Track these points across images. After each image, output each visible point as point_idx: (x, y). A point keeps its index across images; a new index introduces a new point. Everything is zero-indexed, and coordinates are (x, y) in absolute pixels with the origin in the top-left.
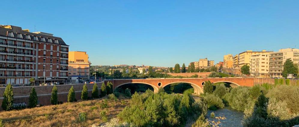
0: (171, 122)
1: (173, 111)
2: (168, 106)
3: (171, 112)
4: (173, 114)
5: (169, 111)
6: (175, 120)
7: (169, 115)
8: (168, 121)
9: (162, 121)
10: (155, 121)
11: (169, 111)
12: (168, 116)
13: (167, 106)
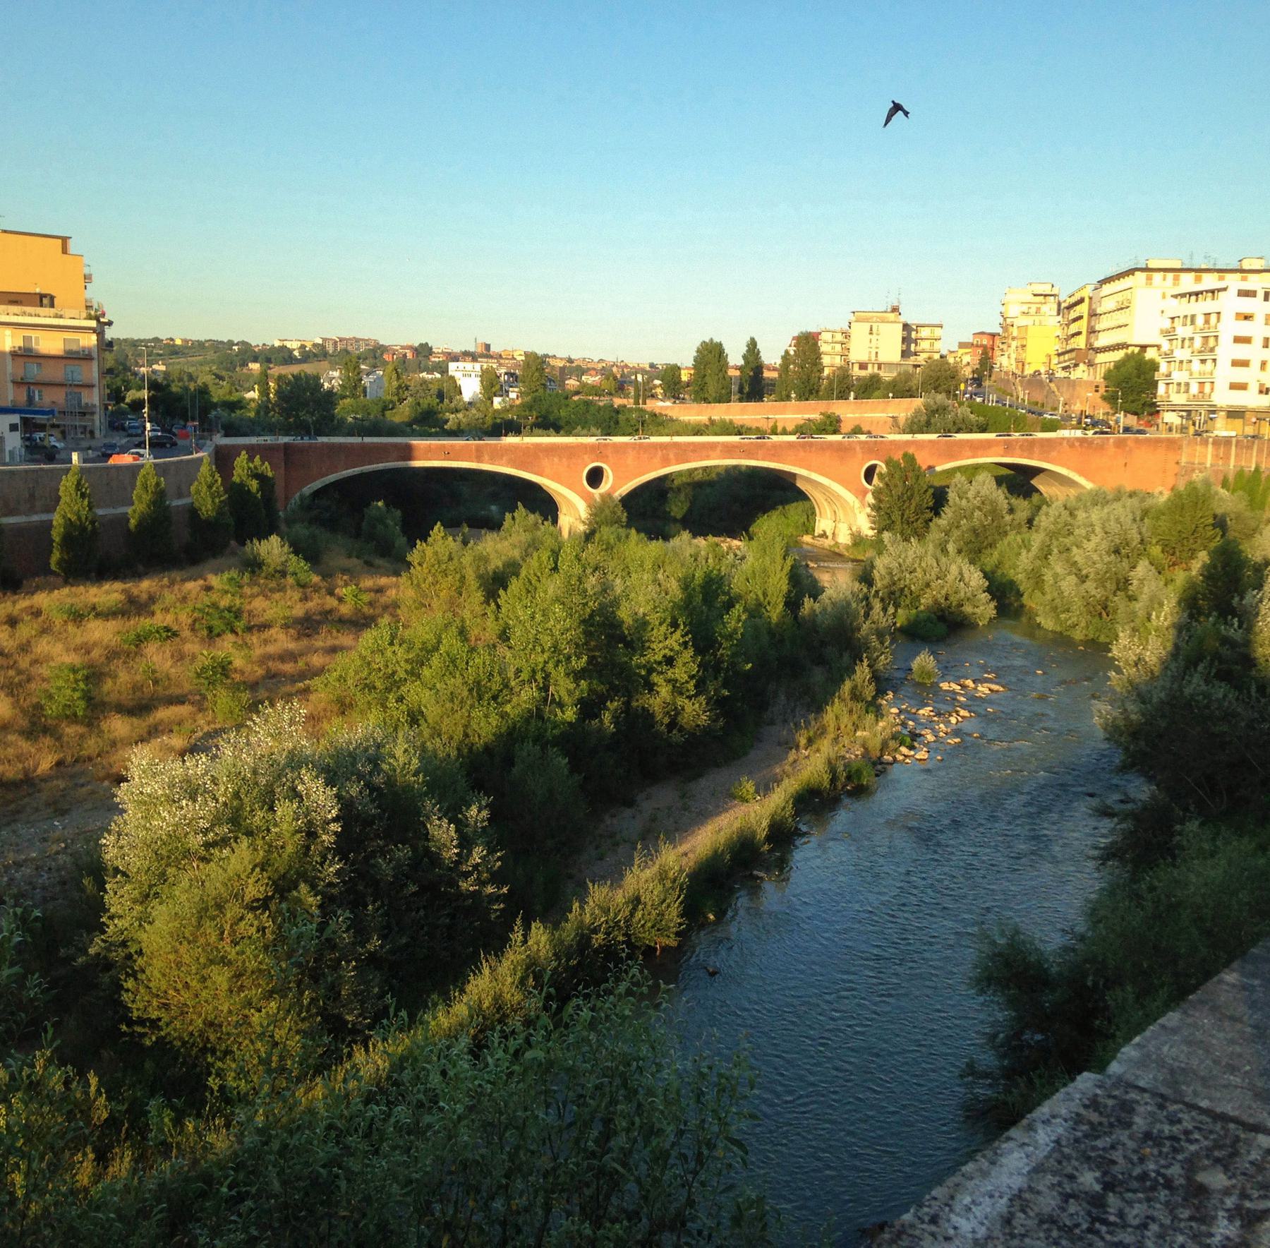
0: (666, 720)
3: (670, 661)
6: (695, 712)
7: (655, 678)
8: (647, 715)
10: (570, 714)
12: (650, 687)
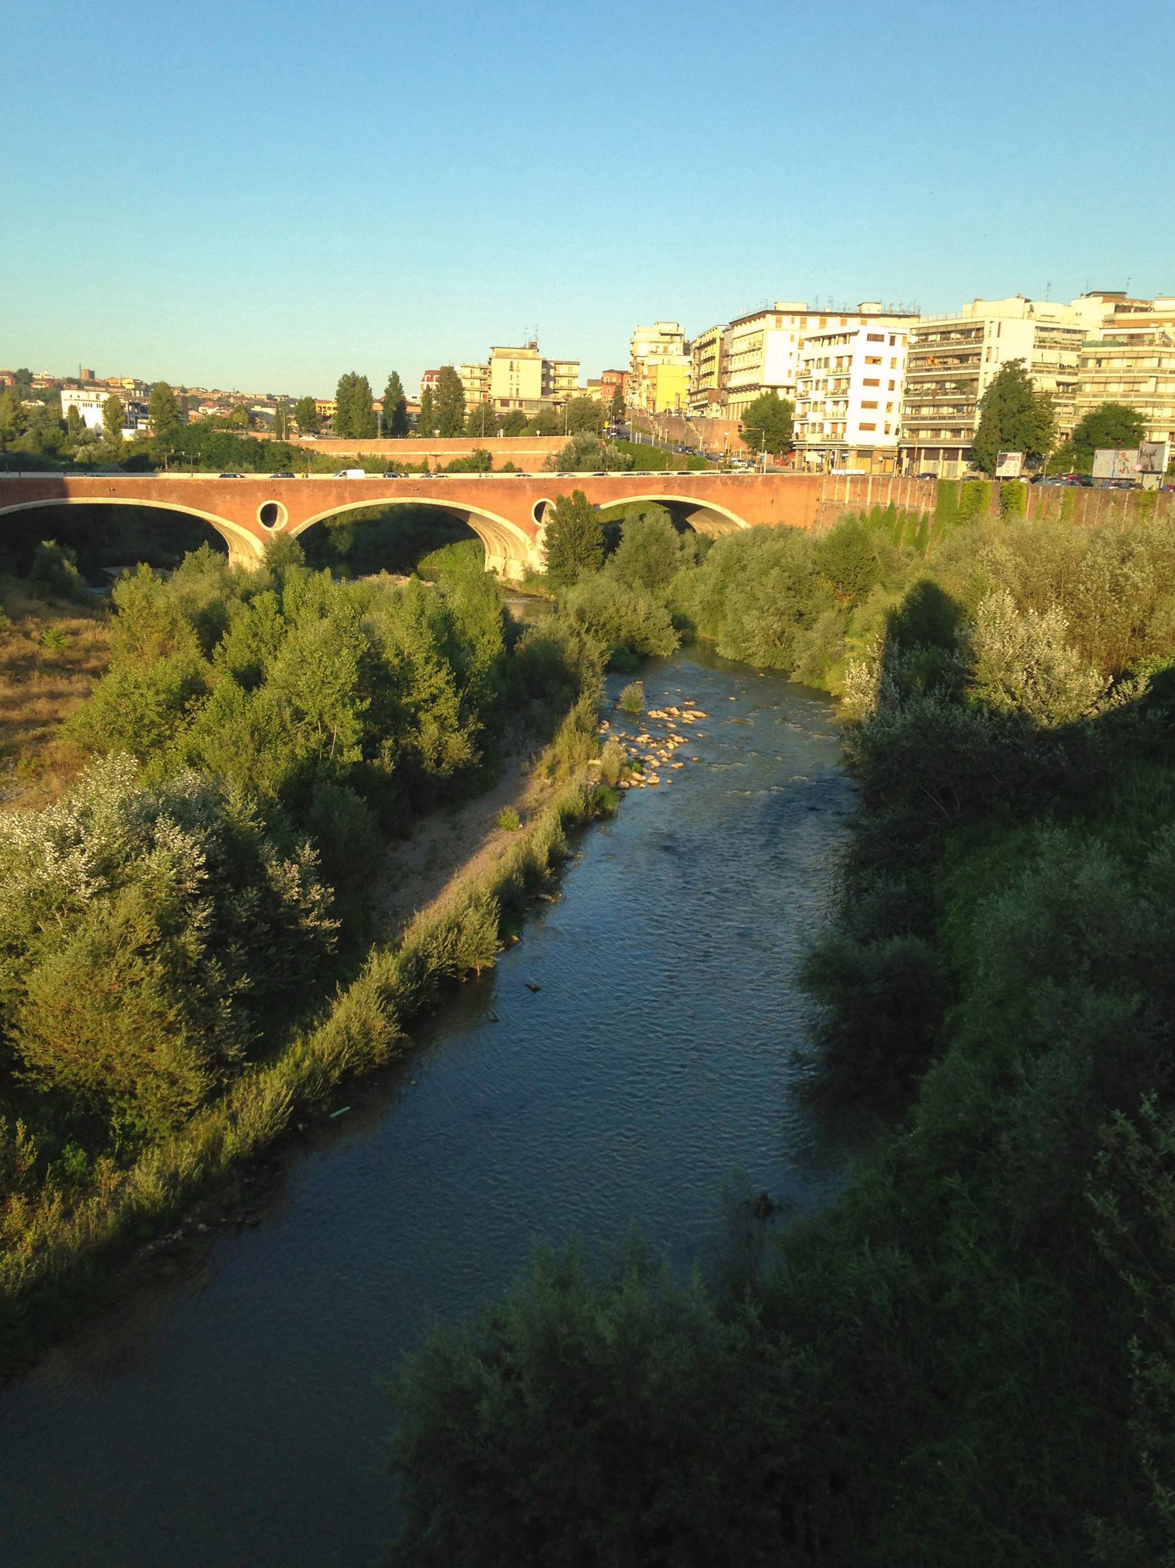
0: (435, 756)
1: (442, 691)
2: (419, 658)
3: (434, 698)
4: (448, 706)
5: (422, 692)
6: (458, 746)
7: (422, 716)
8: (417, 752)
9: (386, 762)
10: (356, 755)
11: (422, 692)
12: (416, 723)
13: (408, 665)
